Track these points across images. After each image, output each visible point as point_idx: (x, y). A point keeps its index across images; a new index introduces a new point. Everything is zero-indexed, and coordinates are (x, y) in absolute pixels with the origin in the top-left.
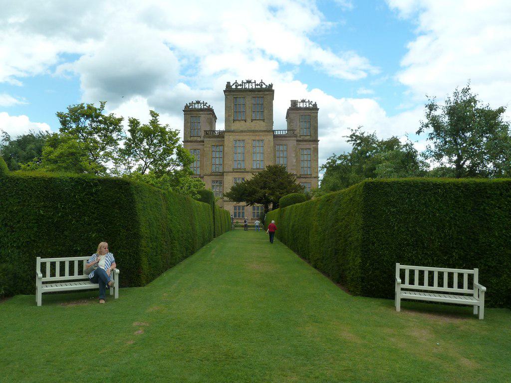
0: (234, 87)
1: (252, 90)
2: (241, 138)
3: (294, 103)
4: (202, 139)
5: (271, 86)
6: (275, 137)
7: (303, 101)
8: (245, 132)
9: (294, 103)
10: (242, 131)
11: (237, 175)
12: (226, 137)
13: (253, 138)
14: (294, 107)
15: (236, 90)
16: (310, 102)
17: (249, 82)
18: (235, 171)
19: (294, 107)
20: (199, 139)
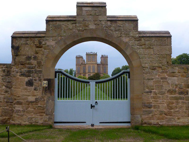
0: (88, 54)
1: (92, 54)
2: (89, 65)
3: (102, 56)
4: (80, 64)
5: (96, 53)
6: (97, 64)
7: (104, 55)
8: (91, 64)
9: (102, 56)
10: (90, 64)
11: (89, 74)
12: (86, 65)
13: (92, 65)
14: (102, 57)
15: (89, 54)
16: (106, 56)
17: (91, 52)
18: (88, 73)
19: (102, 57)
20: (80, 64)
